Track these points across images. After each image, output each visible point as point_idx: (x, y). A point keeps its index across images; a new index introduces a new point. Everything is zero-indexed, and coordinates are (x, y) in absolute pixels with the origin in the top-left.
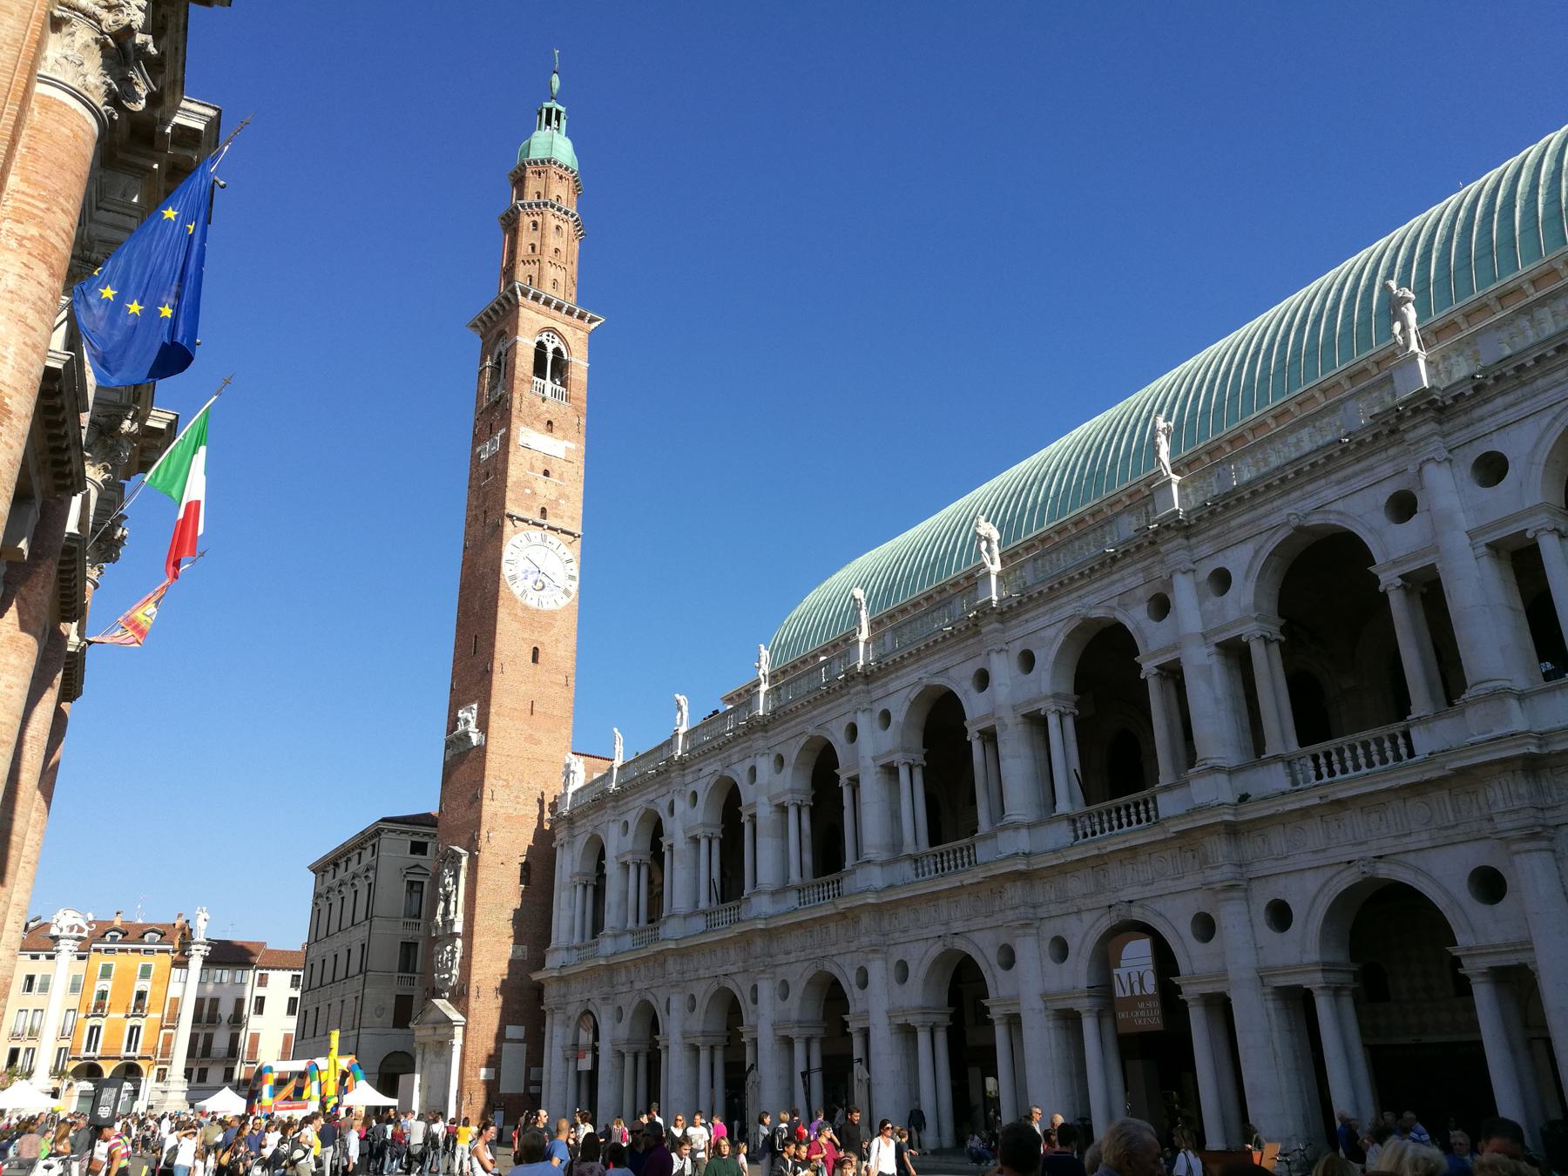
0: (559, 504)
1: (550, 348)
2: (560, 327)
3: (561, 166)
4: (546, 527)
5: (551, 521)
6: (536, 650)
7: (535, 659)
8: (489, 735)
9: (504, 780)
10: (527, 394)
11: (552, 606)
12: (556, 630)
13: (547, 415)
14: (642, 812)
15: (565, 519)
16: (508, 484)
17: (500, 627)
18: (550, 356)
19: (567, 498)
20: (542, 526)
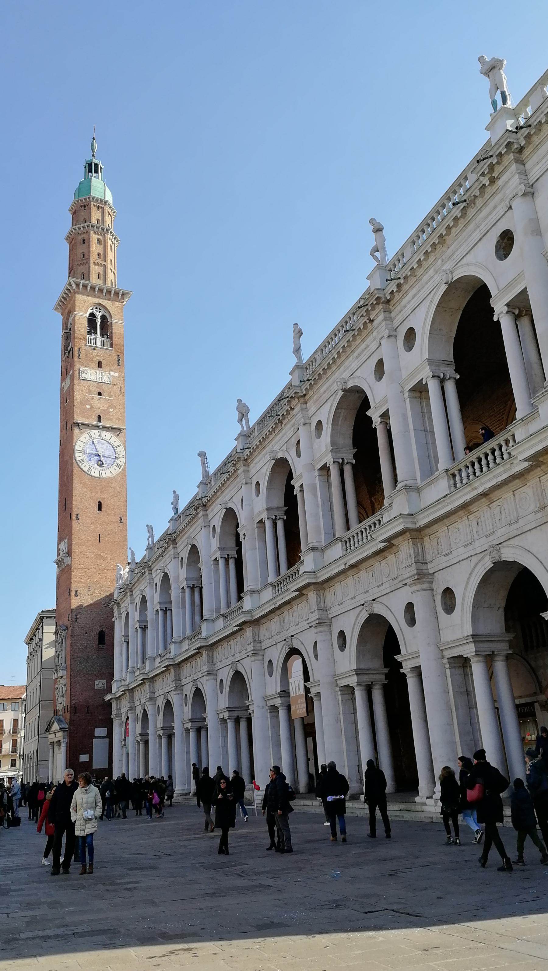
0: (109, 412)
1: (99, 315)
2: (104, 302)
3: (97, 200)
4: (101, 427)
5: (103, 423)
6: (100, 504)
7: (100, 509)
8: (73, 557)
9: (85, 583)
10: (83, 347)
11: (109, 475)
12: (111, 490)
13: (98, 358)
14: (141, 596)
15: (114, 420)
16: (75, 404)
17: (75, 492)
18: (99, 321)
19: (114, 407)
20: (98, 427)
